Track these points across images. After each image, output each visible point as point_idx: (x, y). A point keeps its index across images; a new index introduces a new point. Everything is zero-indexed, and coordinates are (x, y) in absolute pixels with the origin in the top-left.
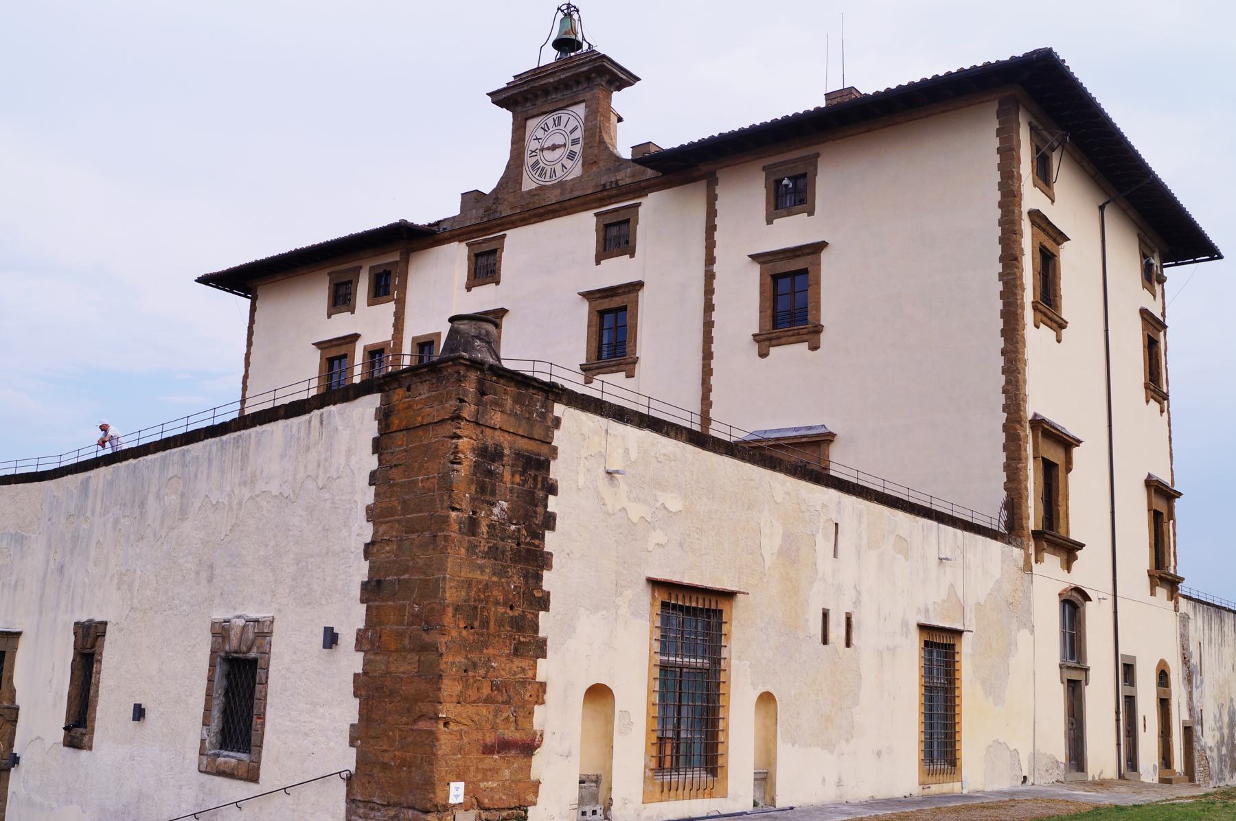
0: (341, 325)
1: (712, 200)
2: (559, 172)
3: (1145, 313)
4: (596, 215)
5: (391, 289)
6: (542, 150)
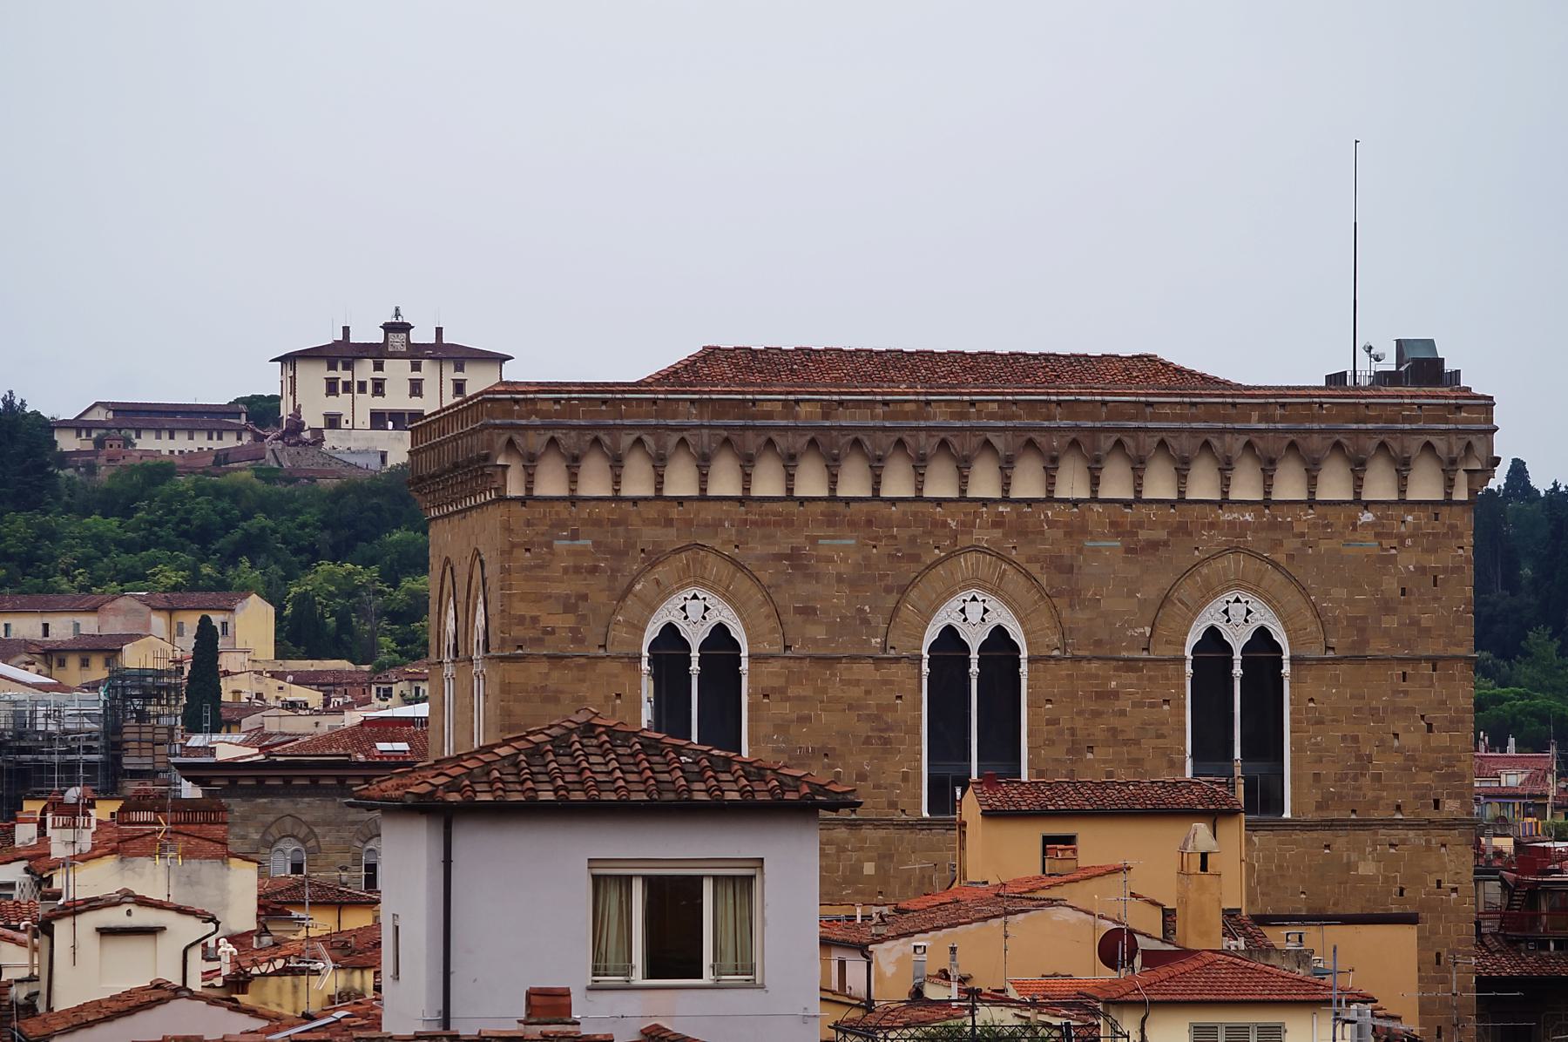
0: (332, 374)
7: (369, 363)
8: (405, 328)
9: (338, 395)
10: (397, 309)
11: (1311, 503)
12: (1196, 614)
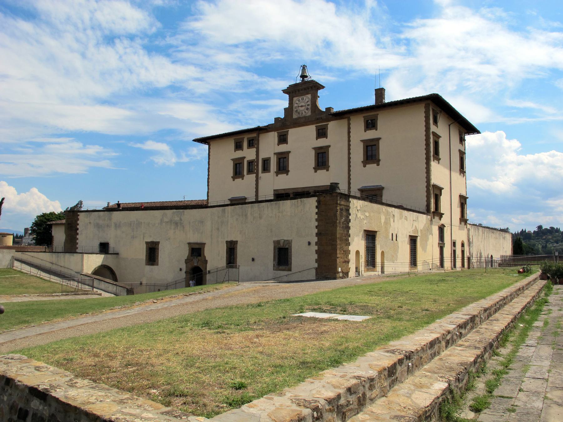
0: (239, 154)
1: (349, 124)
2: (304, 113)
3: (460, 151)
4: (316, 126)
5: (254, 144)
6: (298, 107)
7: (273, 137)
8: (315, 87)
9: (242, 177)
10: (304, 68)
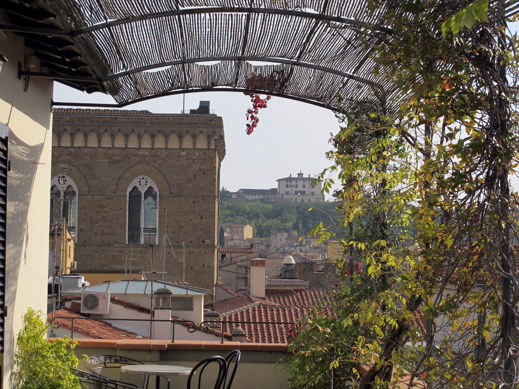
0: (287, 183)
8: (302, 174)
11: (166, 149)
12: (130, 182)
